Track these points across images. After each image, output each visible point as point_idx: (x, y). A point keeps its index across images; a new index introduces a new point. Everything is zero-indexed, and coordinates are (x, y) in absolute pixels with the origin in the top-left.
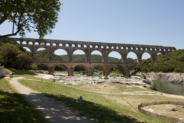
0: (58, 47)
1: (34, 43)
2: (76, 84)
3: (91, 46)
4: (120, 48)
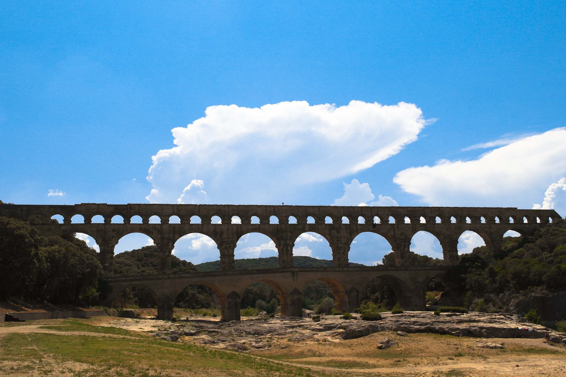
0: (187, 227)
1: (108, 218)
3: (293, 220)
4: (384, 221)
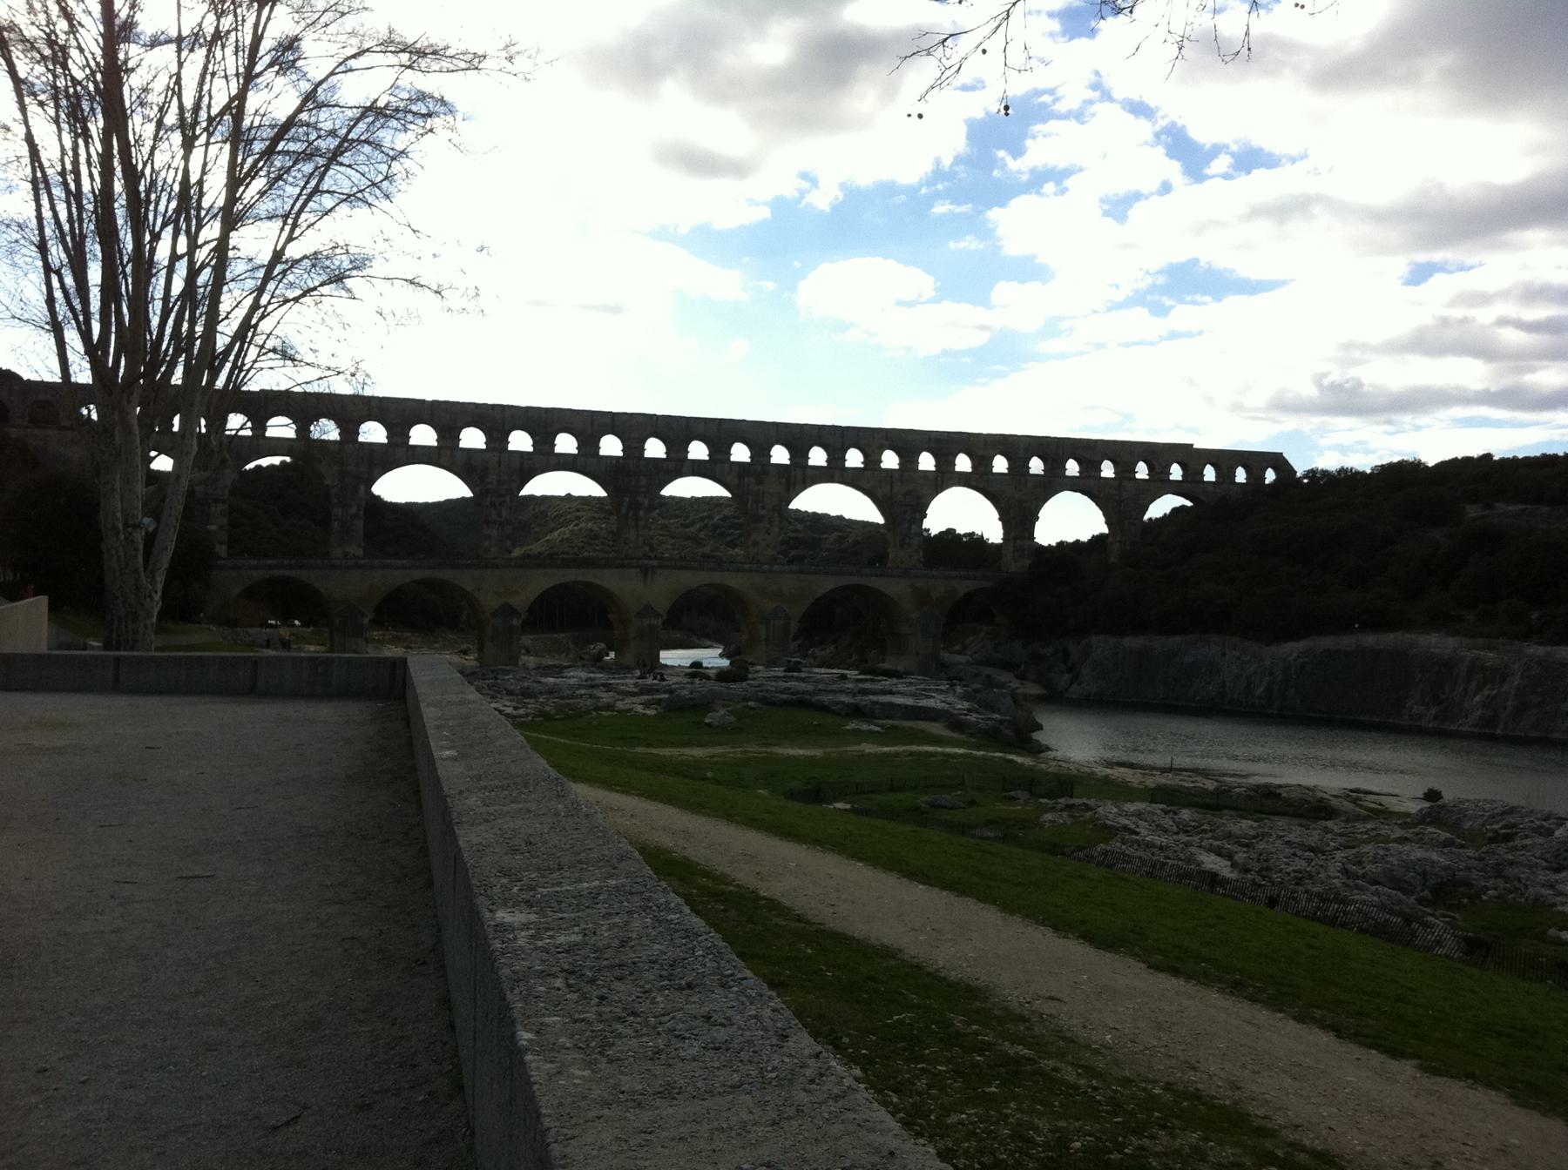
2: (522, 711)
3: (655, 449)
4: (872, 460)
